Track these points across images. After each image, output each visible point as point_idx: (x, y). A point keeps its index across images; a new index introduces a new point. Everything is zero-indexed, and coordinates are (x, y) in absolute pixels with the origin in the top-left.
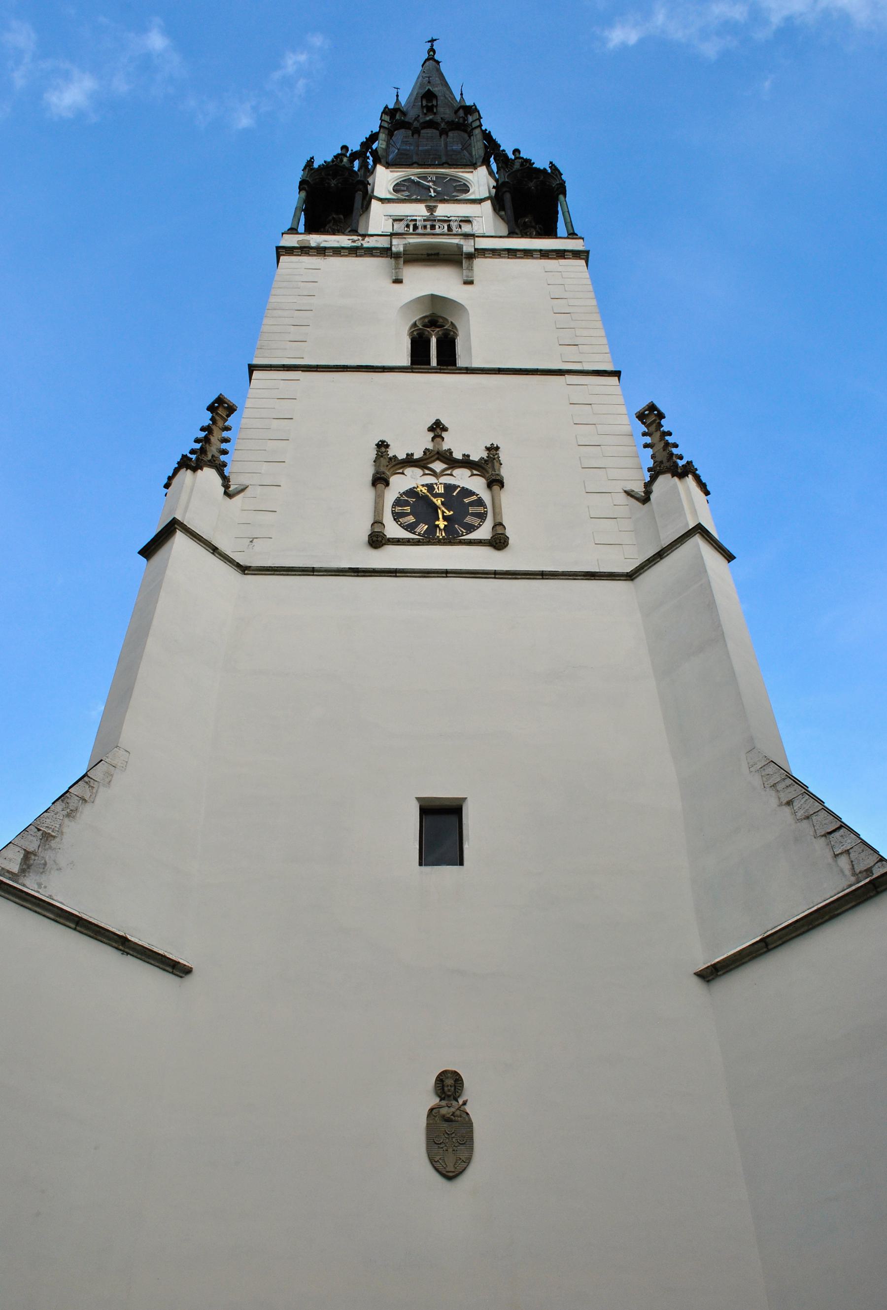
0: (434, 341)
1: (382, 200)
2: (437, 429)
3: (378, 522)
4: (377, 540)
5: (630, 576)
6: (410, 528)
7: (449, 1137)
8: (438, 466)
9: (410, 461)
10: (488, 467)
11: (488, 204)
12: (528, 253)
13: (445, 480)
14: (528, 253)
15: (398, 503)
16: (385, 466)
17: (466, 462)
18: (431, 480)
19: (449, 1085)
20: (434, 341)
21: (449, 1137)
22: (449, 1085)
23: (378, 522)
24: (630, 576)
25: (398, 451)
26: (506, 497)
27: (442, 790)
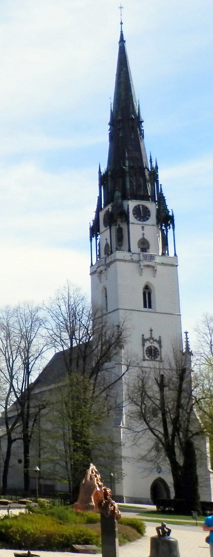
0: (147, 294)
2: (151, 331)
3: (144, 357)
4: (144, 360)
6: (148, 357)
8: (152, 341)
9: (148, 340)
10: (159, 342)
13: (153, 345)
15: (146, 351)
16: (144, 341)
17: (156, 340)
18: (150, 345)
20: (147, 294)
23: (144, 357)
25: (145, 337)
26: (162, 349)
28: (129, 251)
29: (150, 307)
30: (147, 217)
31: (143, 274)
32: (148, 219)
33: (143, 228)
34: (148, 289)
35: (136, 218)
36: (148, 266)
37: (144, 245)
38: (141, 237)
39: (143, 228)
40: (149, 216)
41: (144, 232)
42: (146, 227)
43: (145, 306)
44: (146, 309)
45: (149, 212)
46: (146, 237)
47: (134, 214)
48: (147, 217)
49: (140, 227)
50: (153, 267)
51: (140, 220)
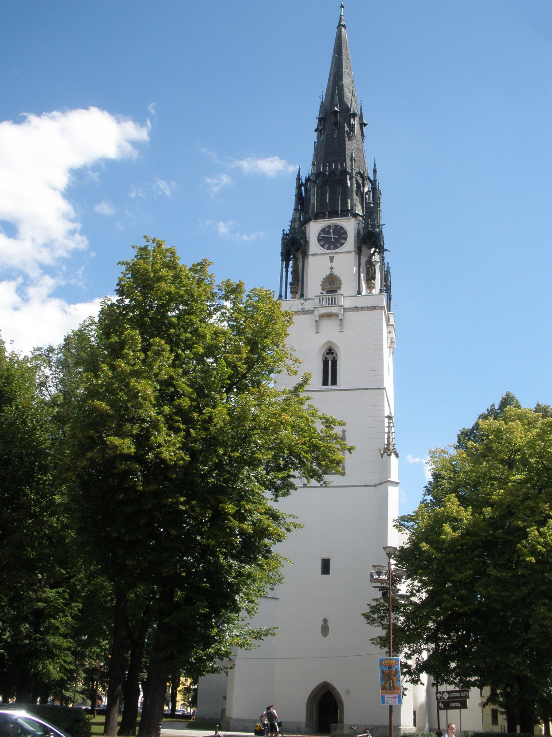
0: (330, 362)
1: (314, 255)
5: (375, 486)
7: (325, 630)
11: (353, 254)
12: (363, 308)
14: (363, 308)
19: (325, 621)
20: (330, 362)
21: (325, 630)
22: (325, 621)
24: (375, 486)
27: (326, 557)
28: (302, 296)
29: (334, 382)
30: (342, 241)
31: (321, 330)
32: (342, 244)
33: (332, 259)
34: (333, 353)
35: (322, 246)
36: (329, 315)
37: (332, 284)
38: (327, 272)
39: (332, 259)
40: (345, 239)
41: (330, 265)
42: (336, 256)
43: (325, 383)
44: (330, 387)
45: (345, 233)
46: (335, 272)
47: (319, 241)
48: (342, 241)
49: (327, 258)
50: (336, 315)
51: (329, 248)
